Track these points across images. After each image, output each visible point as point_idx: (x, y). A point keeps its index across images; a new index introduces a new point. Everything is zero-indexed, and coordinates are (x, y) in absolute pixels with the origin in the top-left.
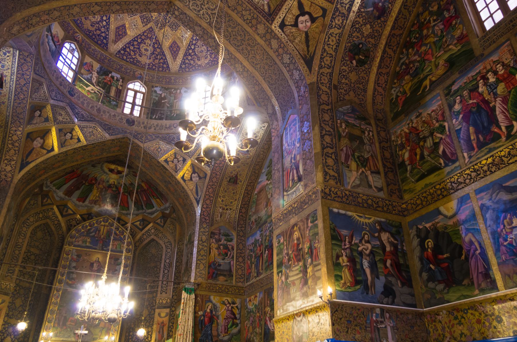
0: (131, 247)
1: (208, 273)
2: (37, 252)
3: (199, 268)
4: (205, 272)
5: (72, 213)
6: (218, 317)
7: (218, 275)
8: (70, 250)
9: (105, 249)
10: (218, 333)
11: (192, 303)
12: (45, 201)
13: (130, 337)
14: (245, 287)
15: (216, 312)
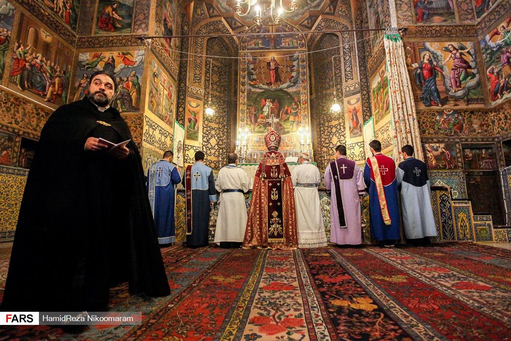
0: (303, 41)
1: (416, 15)
2: (219, 64)
3: (401, 10)
4: (411, 13)
5: (240, 25)
6: (442, 68)
7: (430, 16)
8: (245, 54)
9: (277, 47)
10: (446, 89)
11: (401, 51)
12: (211, 12)
13: (322, 132)
14: (479, 23)
15: (437, 63)
